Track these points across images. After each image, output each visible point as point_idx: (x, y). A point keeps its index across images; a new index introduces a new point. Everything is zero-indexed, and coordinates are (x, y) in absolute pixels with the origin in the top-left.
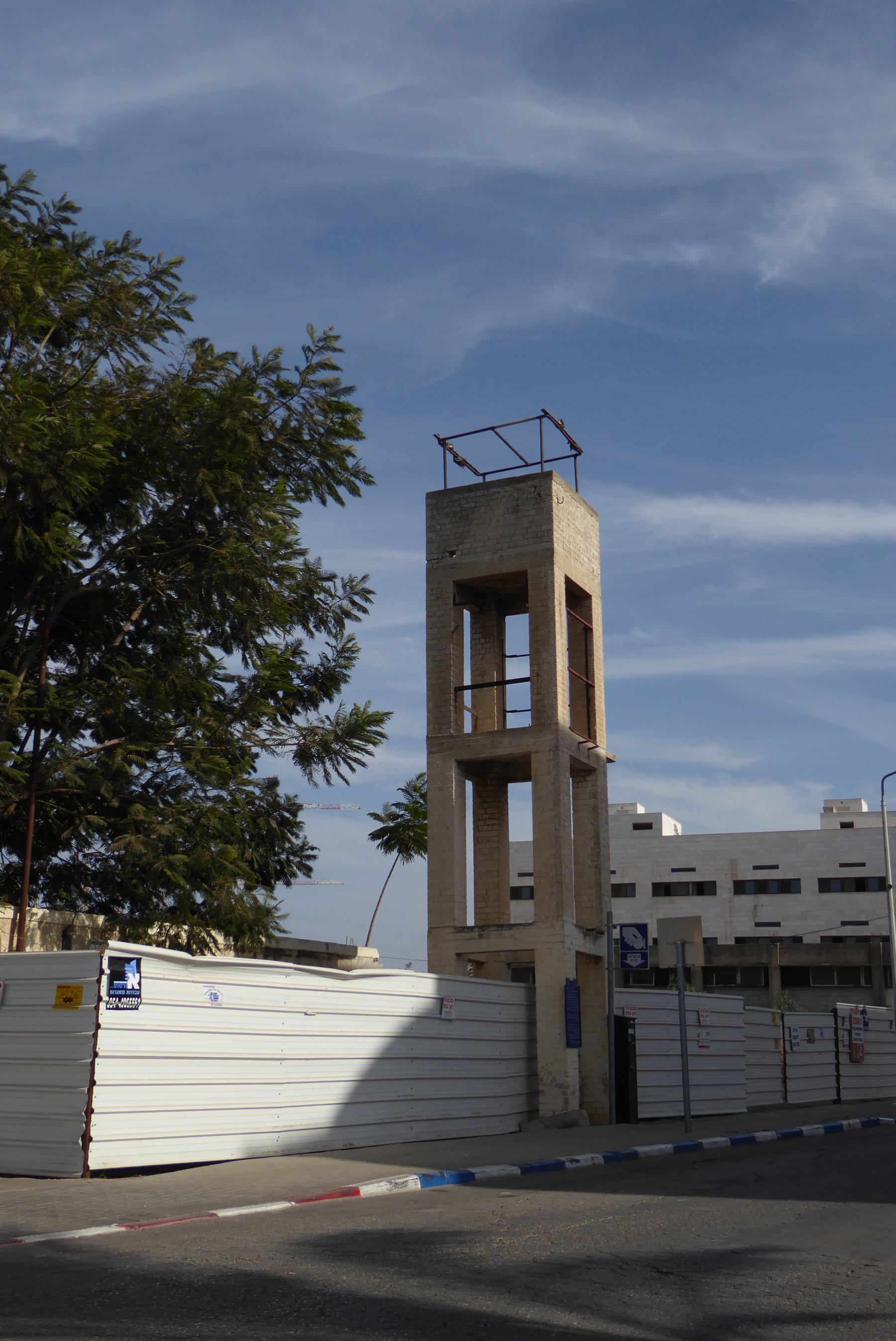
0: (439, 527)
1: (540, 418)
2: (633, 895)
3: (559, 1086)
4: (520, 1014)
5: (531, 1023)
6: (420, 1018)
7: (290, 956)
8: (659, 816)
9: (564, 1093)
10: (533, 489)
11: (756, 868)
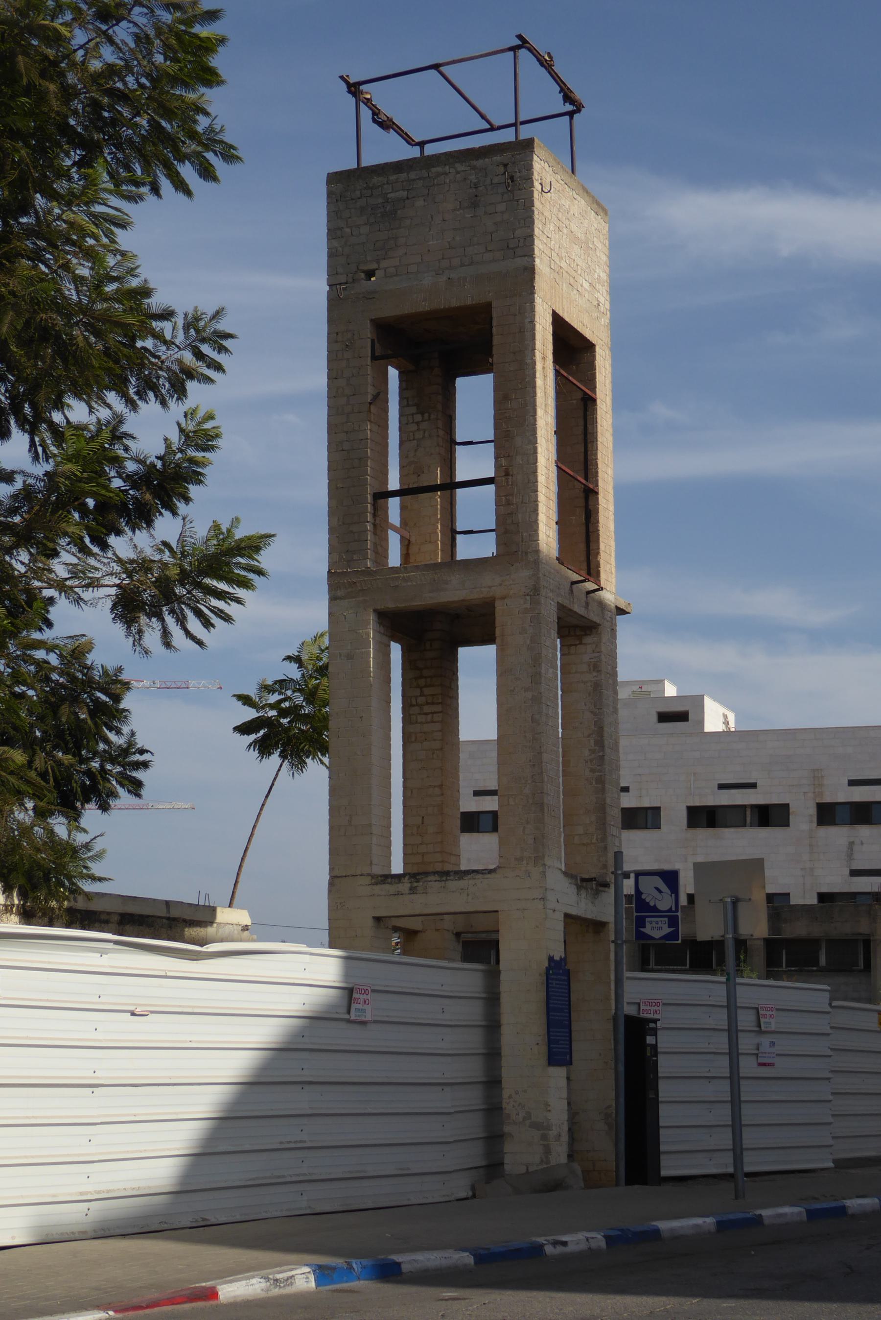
0: (348, 230)
1: (514, 49)
2: (657, 826)
3: (536, 1126)
4: (474, 1012)
5: (492, 1026)
6: (316, 1020)
7: (107, 922)
8: (698, 702)
9: (544, 1137)
10: (502, 169)
11: (852, 783)
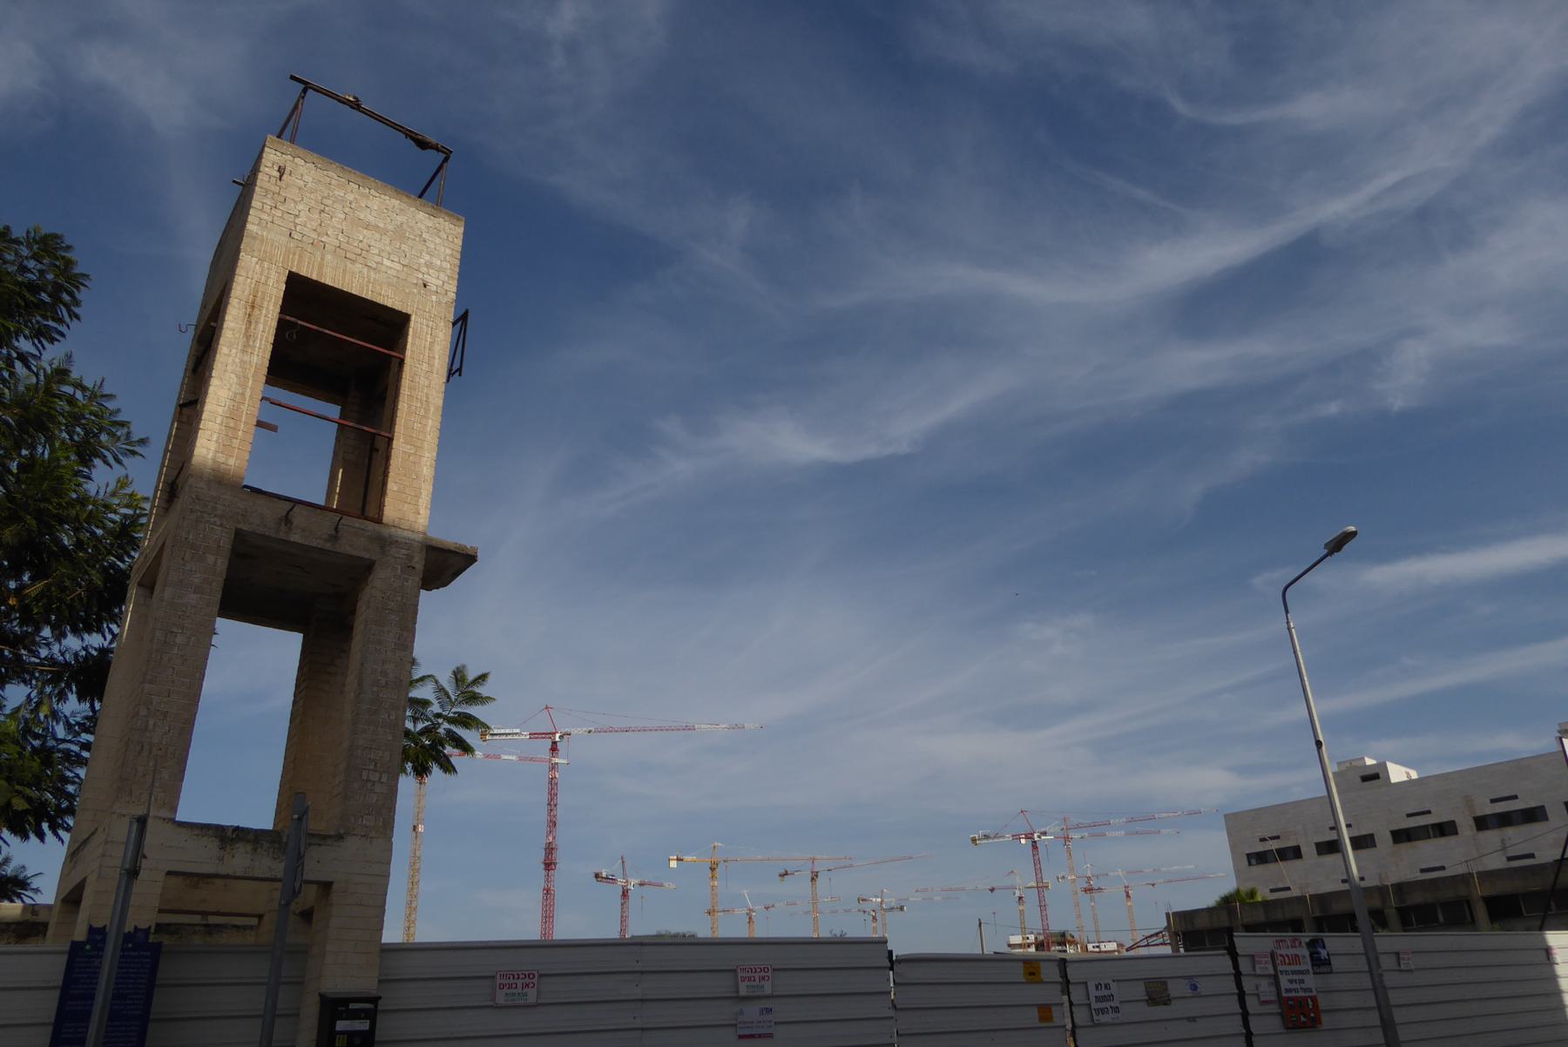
11: (1493, 801)
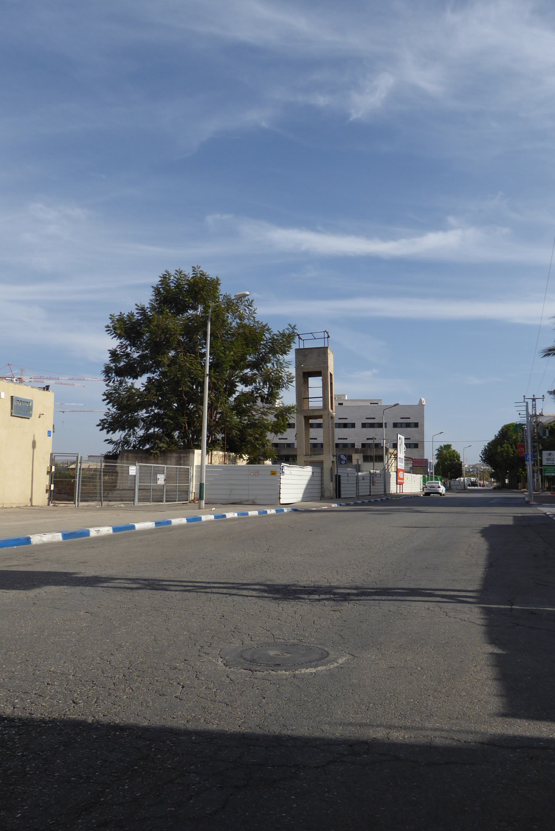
5: (322, 476)
